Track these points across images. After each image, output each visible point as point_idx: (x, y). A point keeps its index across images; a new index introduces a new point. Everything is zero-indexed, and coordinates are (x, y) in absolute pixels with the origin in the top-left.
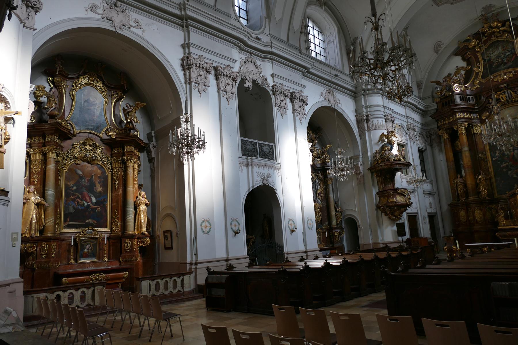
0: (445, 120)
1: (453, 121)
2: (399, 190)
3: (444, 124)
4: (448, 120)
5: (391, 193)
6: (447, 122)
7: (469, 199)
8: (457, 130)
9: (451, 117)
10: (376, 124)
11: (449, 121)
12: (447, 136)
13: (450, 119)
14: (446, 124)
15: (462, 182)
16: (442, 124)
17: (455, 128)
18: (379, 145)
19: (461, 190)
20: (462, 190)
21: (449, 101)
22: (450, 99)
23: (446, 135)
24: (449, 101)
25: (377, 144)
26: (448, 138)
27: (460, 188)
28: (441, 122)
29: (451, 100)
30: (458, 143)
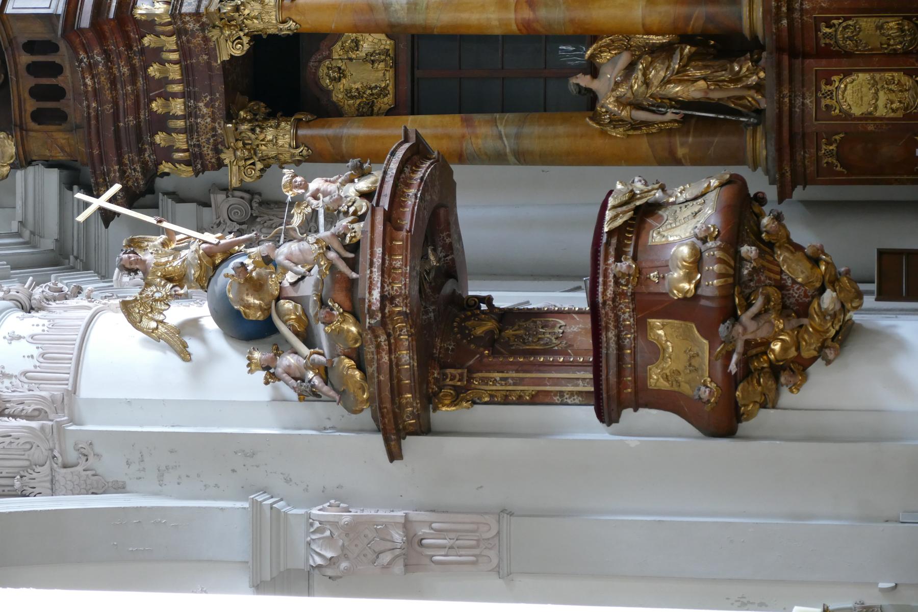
0: (161, 122)
1: (185, 52)
2: (608, 214)
3: (190, 131)
4: (168, 97)
5: (625, 265)
6: (178, 106)
7: (755, 37)
8: (257, 39)
9: (154, 71)
10: (36, 353)
11: (177, 88)
12: (277, 127)
13: (165, 81)
14: (190, 114)
15: (624, 59)
16: (181, 140)
17: (237, 53)
18: (213, 357)
19: (680, 77)
20: (683, 69)
21: (34, 69)
22: (25, 59)
23: (270, 134)
24: (34, 69)
25: (198, 371)
26: (298, 124)
27: (665, 82)
28: (167, 153)
29: (31, 47)
30: (348, 93)
